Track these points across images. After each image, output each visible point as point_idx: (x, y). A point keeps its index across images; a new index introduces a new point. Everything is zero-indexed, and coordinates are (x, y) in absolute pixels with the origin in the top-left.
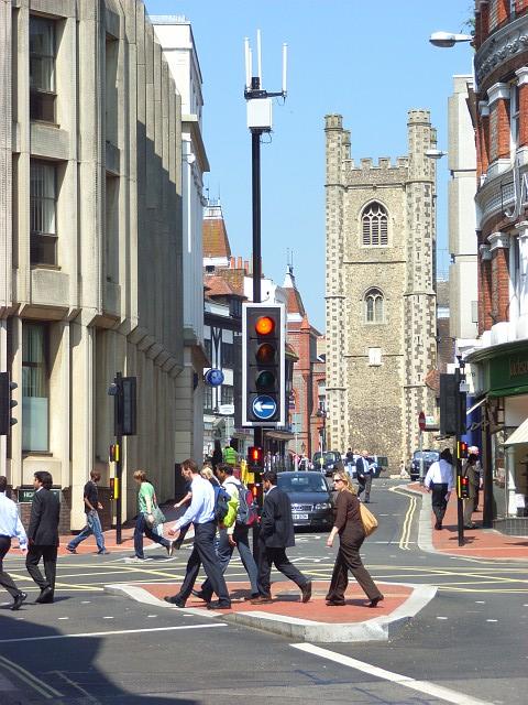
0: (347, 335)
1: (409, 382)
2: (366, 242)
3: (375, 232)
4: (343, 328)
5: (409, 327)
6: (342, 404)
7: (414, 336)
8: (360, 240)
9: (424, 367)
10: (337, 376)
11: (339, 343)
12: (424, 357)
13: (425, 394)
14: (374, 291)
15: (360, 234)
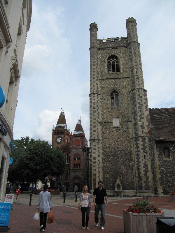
0: (101, 113)
1: (136, 134)
2: (109, 71)
3: (113, 67)
4: (98, 108)
5: (135, 106)
6: (99, 148)
7: (138, 109)
8: (106, 71)
9: (145, 126)
11: (97, 115)
12: (145, 120)
13: (146, 141)
14: (114, 91)
15: (106, 67)
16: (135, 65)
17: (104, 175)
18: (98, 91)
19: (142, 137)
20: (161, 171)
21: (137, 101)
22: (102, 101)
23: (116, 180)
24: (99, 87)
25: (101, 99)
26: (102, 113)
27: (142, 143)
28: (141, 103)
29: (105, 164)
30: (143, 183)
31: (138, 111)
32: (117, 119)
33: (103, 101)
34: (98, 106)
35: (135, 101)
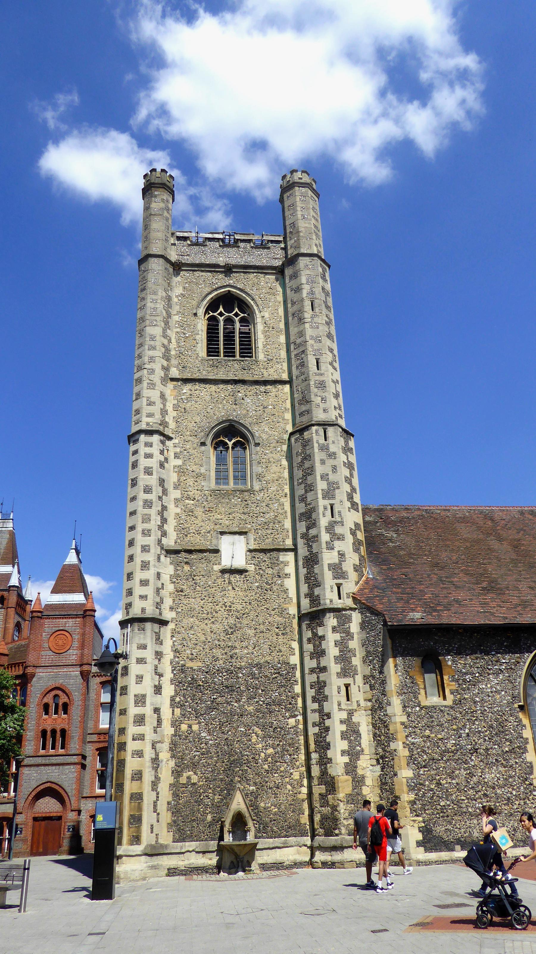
0: (173, 510)
1: (314, 600)
2: (212, 351)
3: (229, 337)
4: (165, 492)
5: (310, 488)
6: (159, 655)
7: (322, 503)
8: (202, 349)
9: (348, 567)
10: (149, 591)
11: (156, 520)
13: (354, 626)
15: (202, 336)
16: (312, 338)
17: (177, 773)
18: (164, 424)
19: (336, 610)
20: (411, 751)
21: (319, 470)
22: (179, 462)
23: (228, 796)
24: (169, 407)
25: (176, 456)
26: (178, 510)
27: (337, 636)
28: (332, 477)
29: (184, 727)
30: (341, 804)
31: (321, 509)
32: (237, 537)
33: (184, 464)
34: (162, 482)
35: (310, 471)
